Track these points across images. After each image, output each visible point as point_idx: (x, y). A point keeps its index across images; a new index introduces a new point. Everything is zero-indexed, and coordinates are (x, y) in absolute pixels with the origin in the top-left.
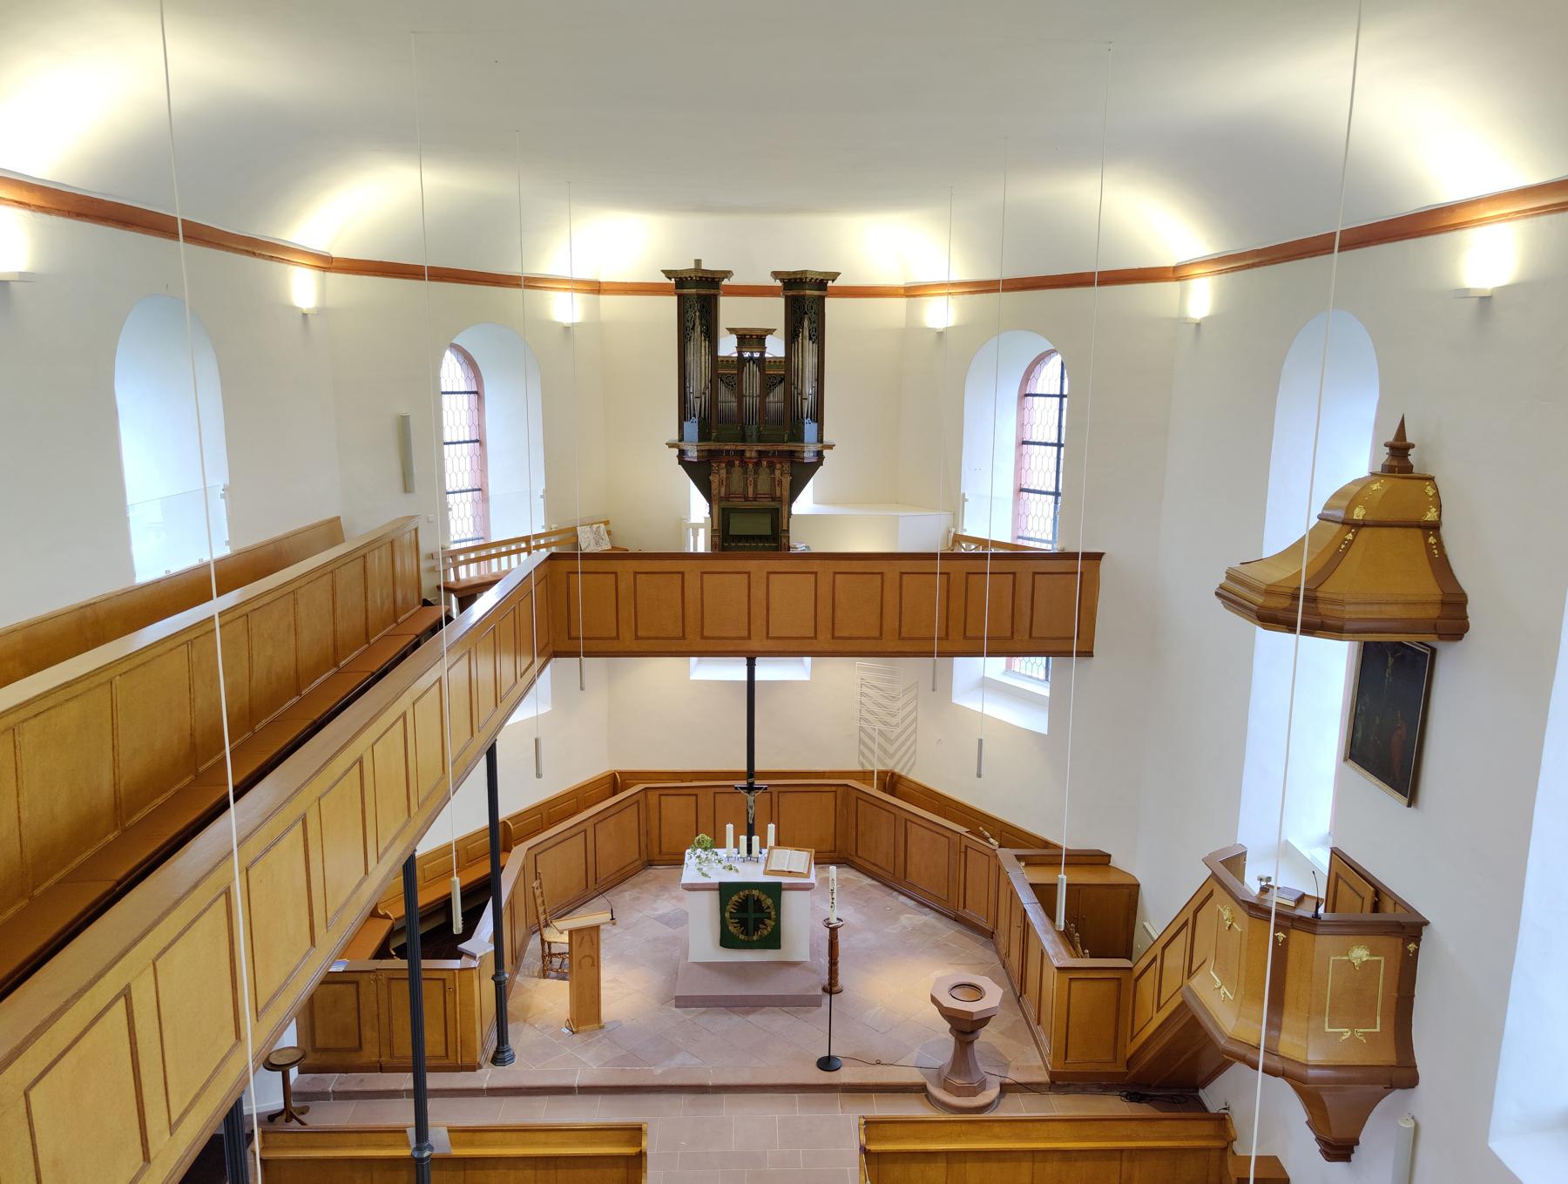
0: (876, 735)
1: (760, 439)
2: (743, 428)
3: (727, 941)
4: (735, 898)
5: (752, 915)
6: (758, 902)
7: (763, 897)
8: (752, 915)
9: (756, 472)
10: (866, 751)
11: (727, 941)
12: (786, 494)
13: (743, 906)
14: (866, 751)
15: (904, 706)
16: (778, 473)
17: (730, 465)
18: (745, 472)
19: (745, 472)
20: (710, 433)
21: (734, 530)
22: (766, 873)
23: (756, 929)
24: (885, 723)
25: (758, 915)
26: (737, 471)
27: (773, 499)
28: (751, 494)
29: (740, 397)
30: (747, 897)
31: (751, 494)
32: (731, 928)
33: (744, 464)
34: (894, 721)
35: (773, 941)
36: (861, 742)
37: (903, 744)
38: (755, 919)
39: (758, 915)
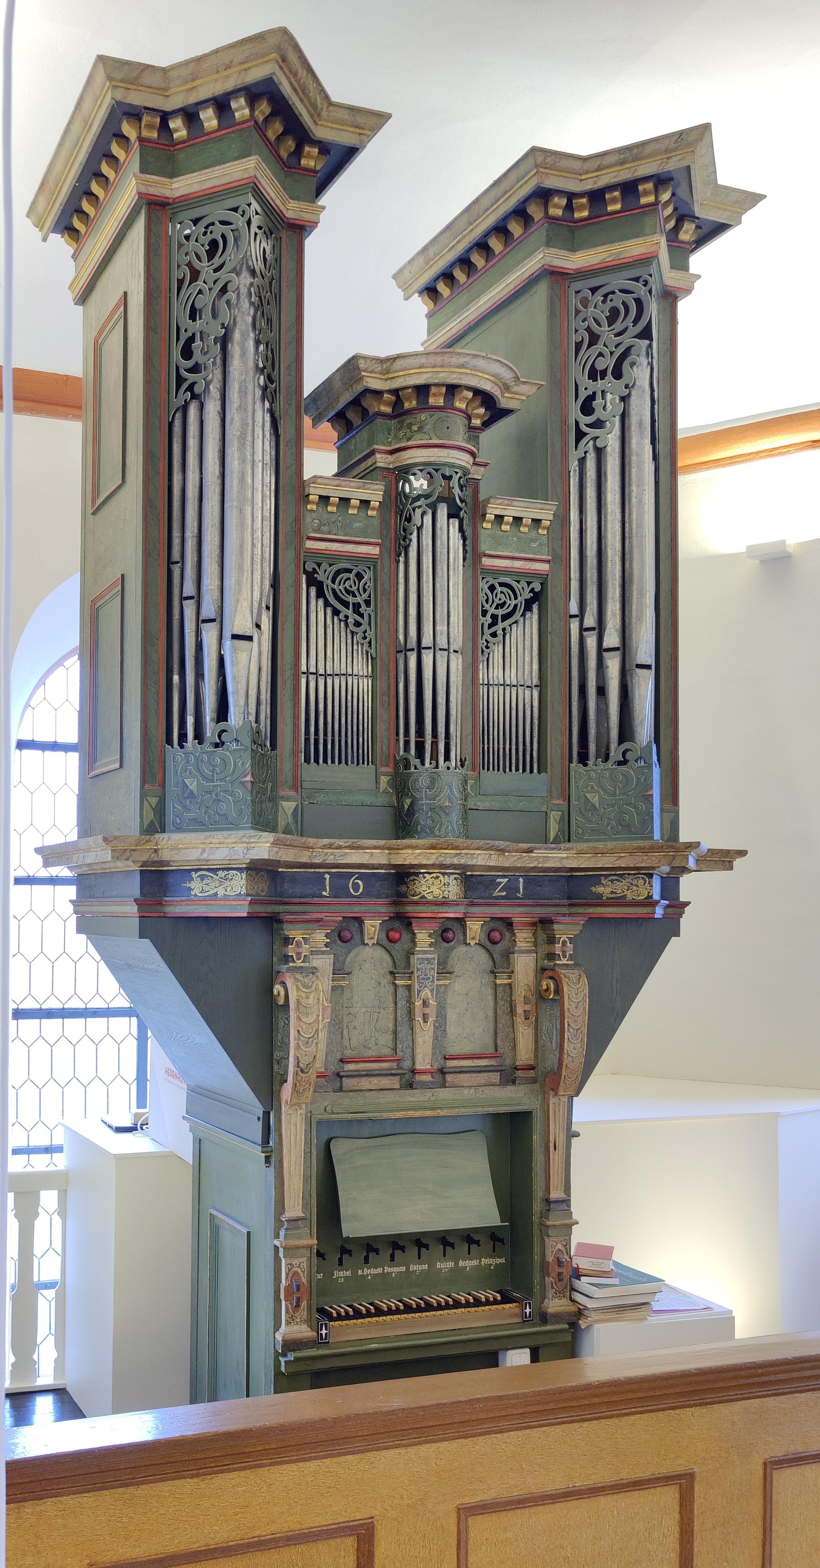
1: (470, 830)
2: (401, 784)
9: (444, 970)
12: (575, 1049)
16: (524, 966)
17: (346, 934)
18: (401, 967)
19: (401, 967)
20: (274, 799)
21: (362, 1217)
26: (370, 959)
27: (509, 1075)
28: (424, 1060)
29: (394, 657)
31: (424, 1060)
33: (401, 922)
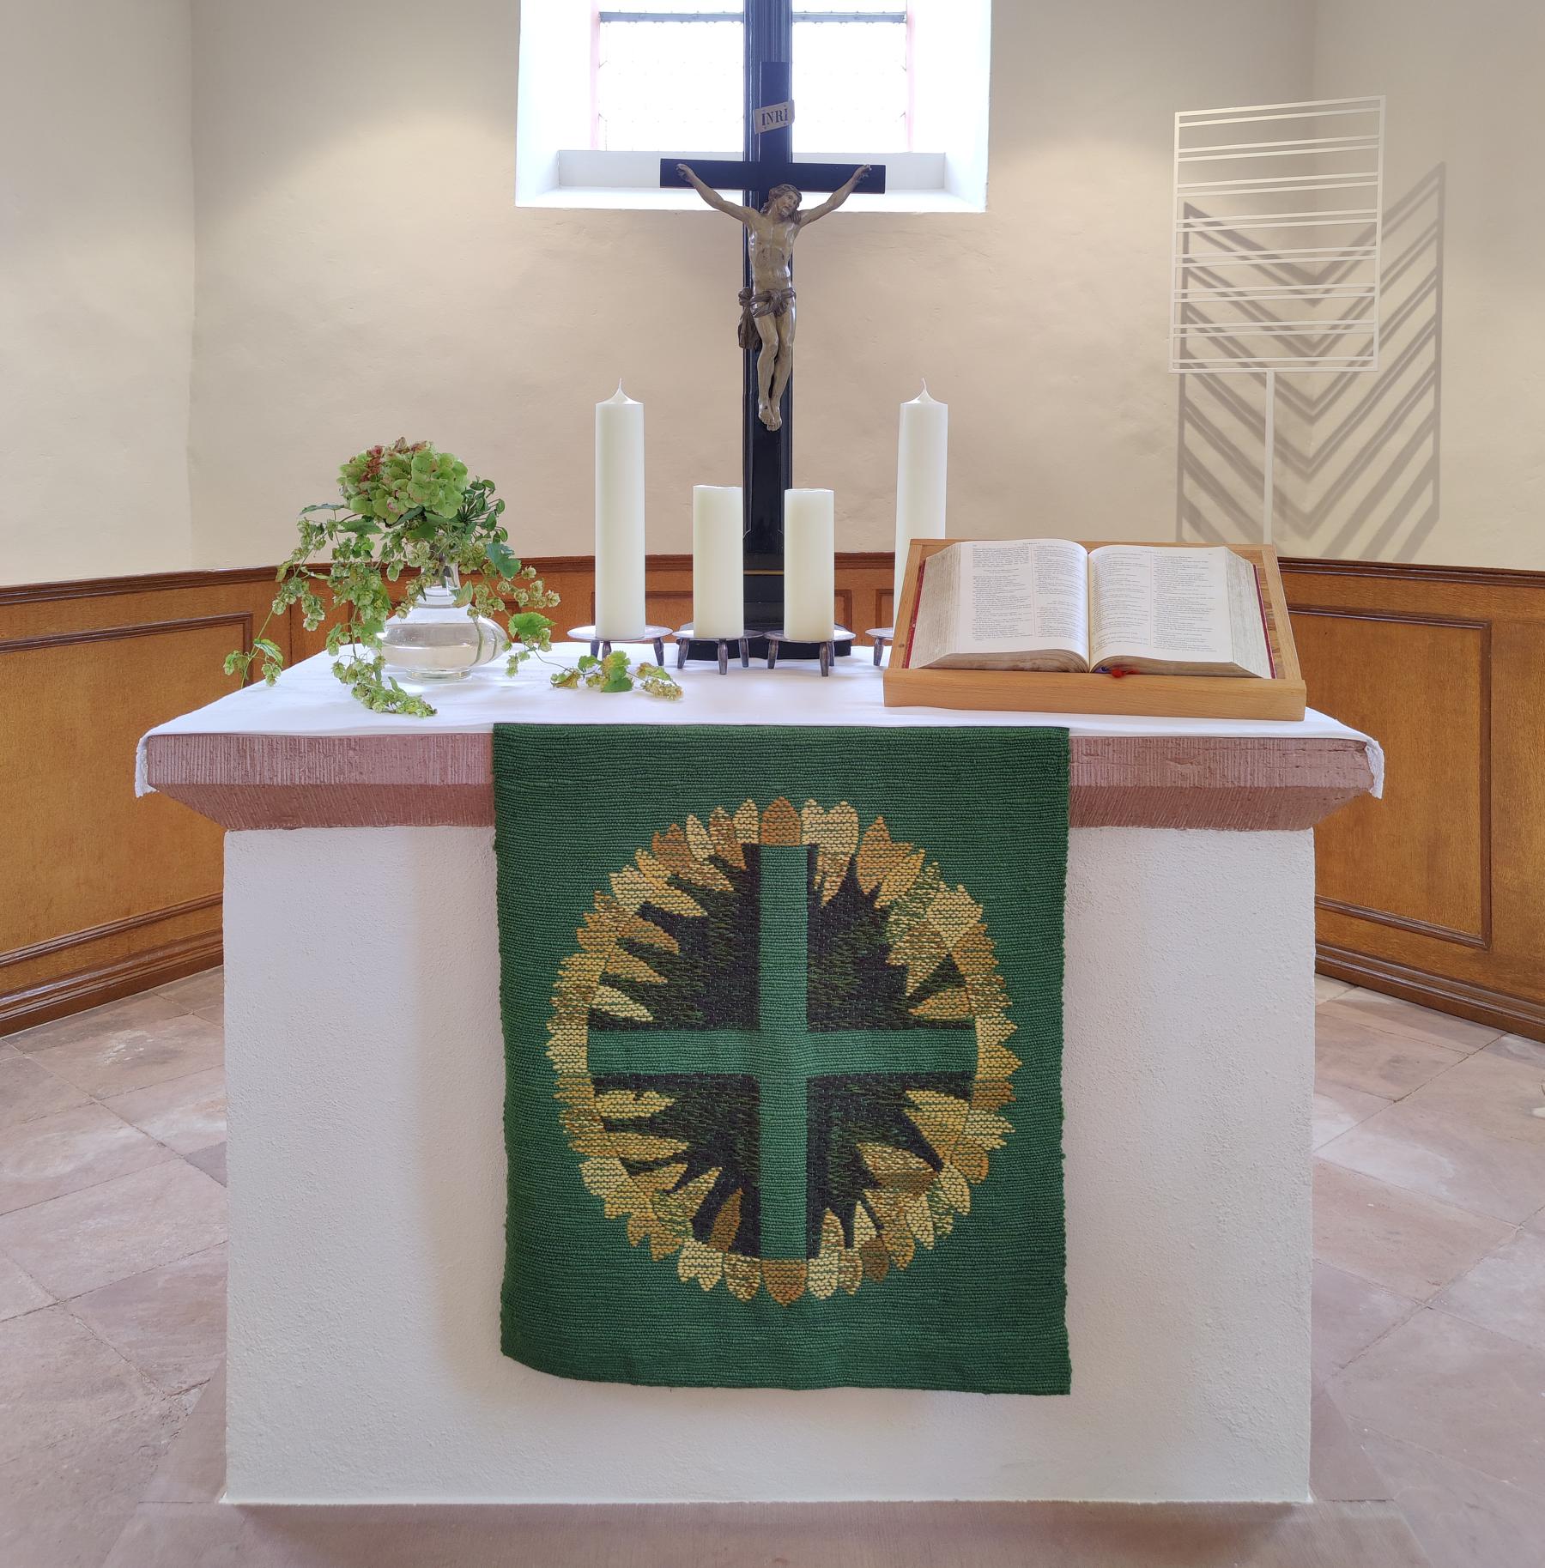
0: (1266, 400)
3: (568, 1308)
4: (640, 882)
5: (797, 1055)
6: (852, 914)
7: (894, 874)
8: (797, 1055)
10: (1204, 502)
11: (568, 1308)
13: (711, 963)
14: (1204, 502)
15: (1390, 277)
22: (896, 697)
23: (837, 1186)
24: (1286, 391)
25: (858, 1052)
30: (750, 870)
32: (603, 1177)
34: (1318, 374)
35: (993, 1312)
36: (1188, 464)
37: (1393, 423)
38: (825, 1090)
39: (858, 1052)
